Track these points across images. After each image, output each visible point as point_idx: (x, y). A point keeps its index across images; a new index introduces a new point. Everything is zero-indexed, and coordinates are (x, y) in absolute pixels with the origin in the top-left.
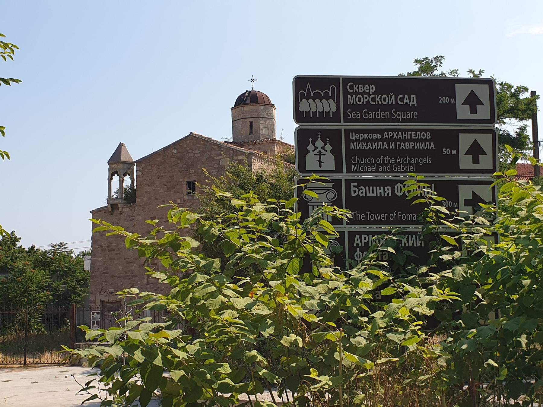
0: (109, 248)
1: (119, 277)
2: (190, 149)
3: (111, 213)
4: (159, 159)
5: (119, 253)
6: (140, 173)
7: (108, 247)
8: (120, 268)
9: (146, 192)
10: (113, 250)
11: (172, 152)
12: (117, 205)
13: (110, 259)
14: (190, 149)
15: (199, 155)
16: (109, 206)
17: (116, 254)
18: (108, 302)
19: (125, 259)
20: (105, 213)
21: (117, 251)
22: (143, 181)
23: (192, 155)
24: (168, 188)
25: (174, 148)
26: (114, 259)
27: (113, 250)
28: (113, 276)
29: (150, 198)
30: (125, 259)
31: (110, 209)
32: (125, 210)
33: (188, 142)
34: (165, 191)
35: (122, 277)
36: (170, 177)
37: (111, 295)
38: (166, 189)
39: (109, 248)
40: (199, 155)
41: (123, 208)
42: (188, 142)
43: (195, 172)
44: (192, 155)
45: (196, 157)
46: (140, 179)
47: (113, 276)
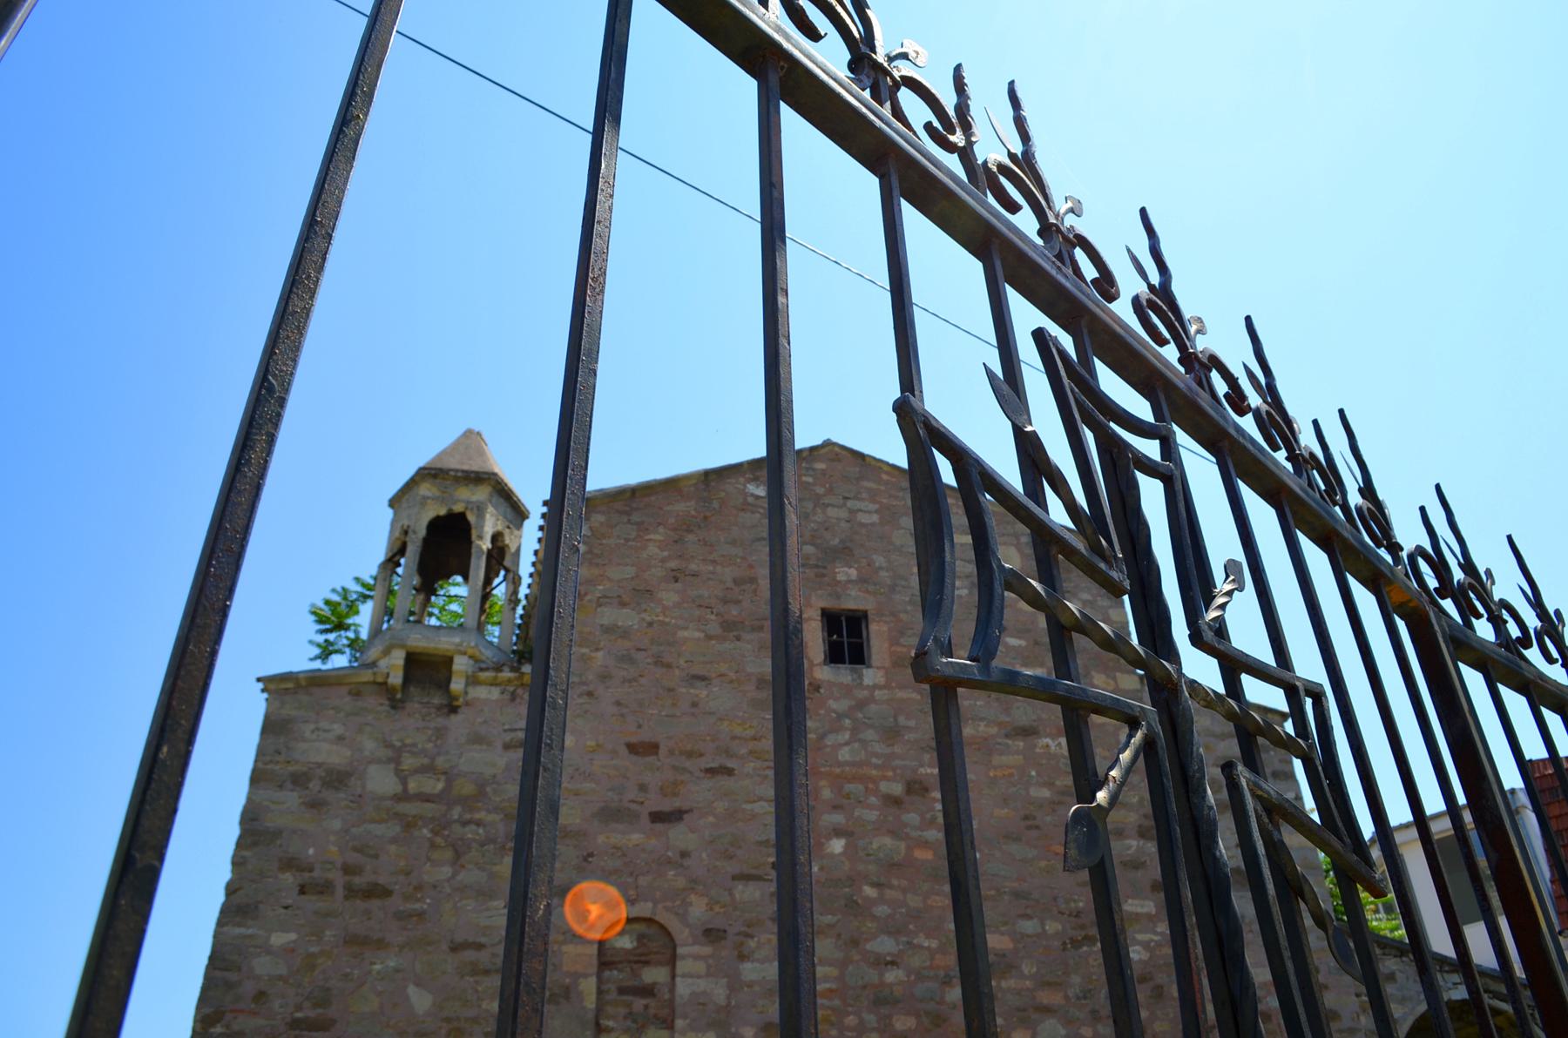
0: (357, 880)
2: (830, 491)
3: (395, 699)
4: (683, 507)
5: (421, 915)
7: (348, 870)
8: (421, 1000)
9: (608, 630)
10: (376, 892)
11: (745, 494)
12: (448, 661)
14: (830, 491)
15: (875, 518)
16: (398, 658)
17: (401, 916)
19: (455, 948)
20: (356, 693)
21: (407, 898)
22: (590, 582)
23: (843, 514)
24: (729, 626)
25: (755, 479)
26: (381, 944)
27: (376, 892)
29: (627, 659)
30: (455, 948)
31: (396, 679)
32: (480, 692)
33: (820, 466)
34: (709, 637)
36: (735, 581)
38: (714, 628)
39: (357, 880)
40: (875, 518)
41: (472, 681)
42: (820, 466)
43: (862, 580)
44: (843, 514)
45: (862, 525)
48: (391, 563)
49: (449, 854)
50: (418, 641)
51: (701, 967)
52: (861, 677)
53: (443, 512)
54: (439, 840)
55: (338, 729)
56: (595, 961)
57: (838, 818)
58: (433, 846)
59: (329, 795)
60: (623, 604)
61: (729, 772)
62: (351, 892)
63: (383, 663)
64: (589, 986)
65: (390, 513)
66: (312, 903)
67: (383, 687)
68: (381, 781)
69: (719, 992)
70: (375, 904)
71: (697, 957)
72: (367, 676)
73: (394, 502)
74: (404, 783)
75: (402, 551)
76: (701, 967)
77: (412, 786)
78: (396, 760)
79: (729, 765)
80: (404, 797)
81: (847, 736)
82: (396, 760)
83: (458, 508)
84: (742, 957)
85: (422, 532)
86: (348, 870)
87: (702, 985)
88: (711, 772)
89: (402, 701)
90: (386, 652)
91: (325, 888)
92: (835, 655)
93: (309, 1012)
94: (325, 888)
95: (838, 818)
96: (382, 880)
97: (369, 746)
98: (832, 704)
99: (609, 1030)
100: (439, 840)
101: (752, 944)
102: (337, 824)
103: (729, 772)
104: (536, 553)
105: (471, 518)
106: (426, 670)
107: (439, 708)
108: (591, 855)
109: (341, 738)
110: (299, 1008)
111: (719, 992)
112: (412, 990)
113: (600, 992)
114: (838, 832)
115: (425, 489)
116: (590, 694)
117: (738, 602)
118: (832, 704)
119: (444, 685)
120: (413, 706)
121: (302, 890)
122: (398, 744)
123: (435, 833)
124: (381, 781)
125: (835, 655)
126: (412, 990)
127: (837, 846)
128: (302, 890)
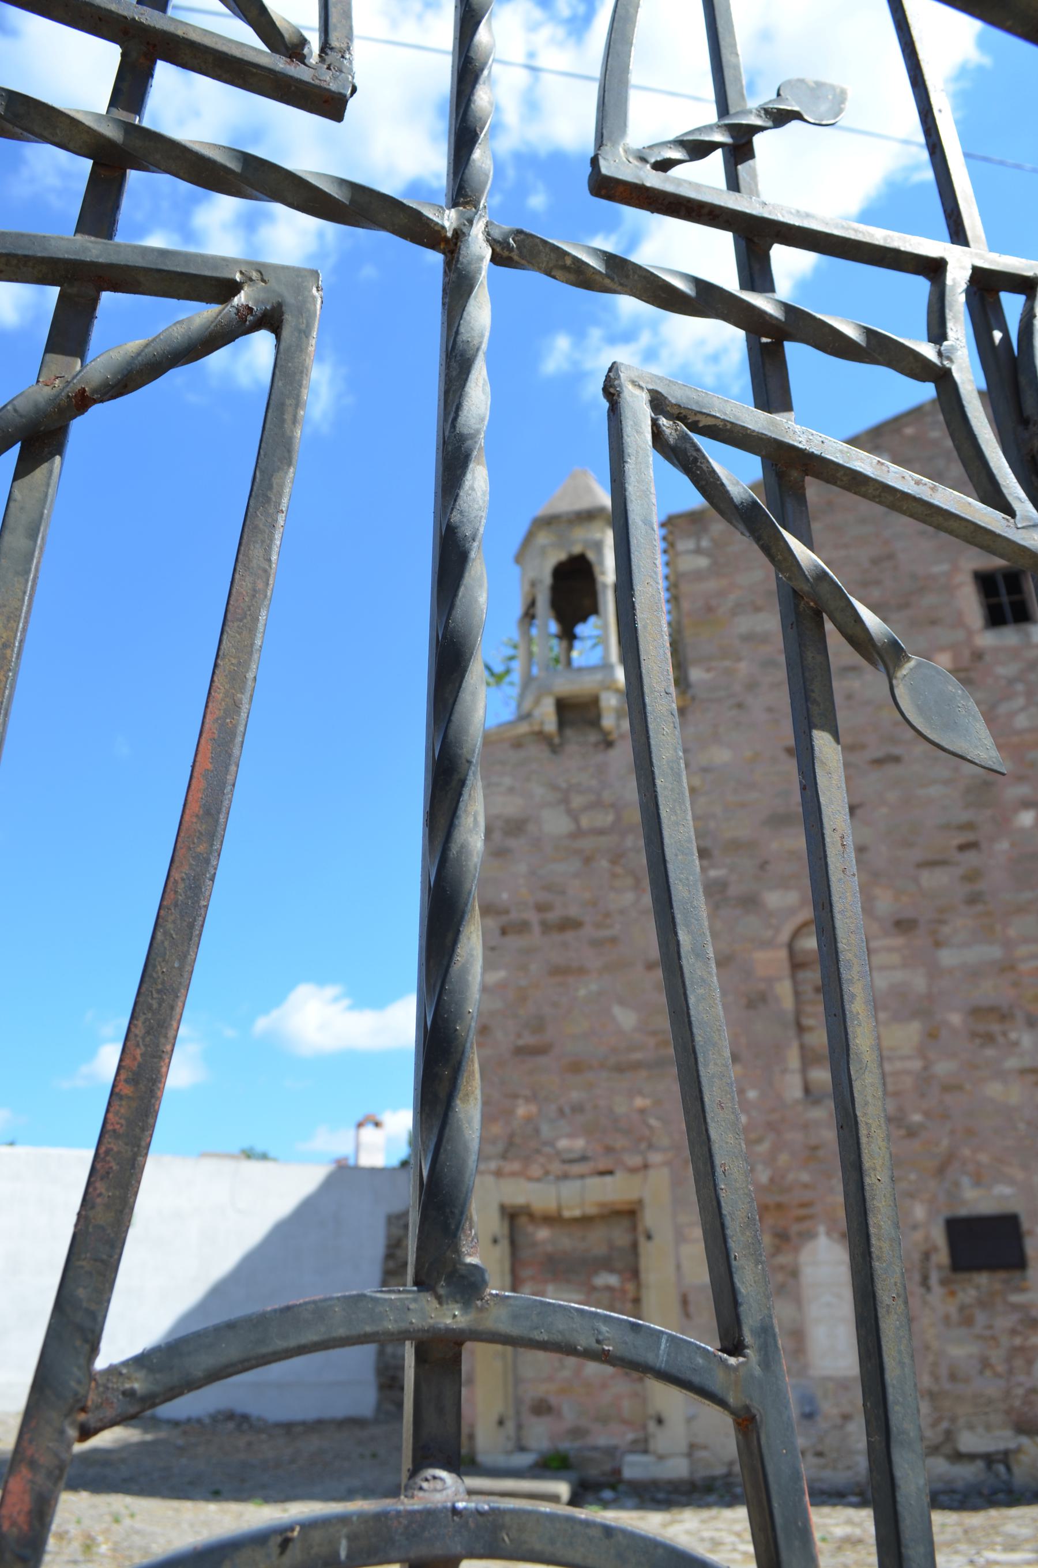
1: (620, 1069)
5: (613, 940)
6: (703, 562)
7: (541, 908)
10: (568, 924)
13: (560, 971)
17: (596, 944)
18: (553, 1220)
21: (598, 926)
26: (581, 971)
27: (568, 924)
28: (576, 1067)
31: (551, 725)
35: (636, 1066)
37: (576, 1169)
46: (712, 585)
47: (576, 1067)
48: (529, 615)
49: (629, 881)
50: (566, 685)
51: (895, 958)
52: (1028, 635)
53: (563, 556)
54: (619, 870)
55: (507, 781)
56: (786, 965)
57: (1023, 790)
58: (614, 876)
59: (512, 843)
60: (757, 609)
61: (896, 759)
62: (547, 928)
63: (537, 713)
64: (784, 990)
65: (515, 571)
66: (514, 942)
67: (541, 736)
68: (555, 823)
69: (919, 982)
70: (569, 936)
71: (890, 950)
72: (523, 728)
73: (519, 558)
74: (576, 819)
75: (532, 604)
76: (895, 958)
77: (585, 822)
78: (565, 801)
79: (897, 751)
80: (578, 833)
81: (1021, 701)
82: (565, 801)
83: (577, 549)
84: (938, 944)
85: (547, 579)
86: (541, 908)
87: (899, 976)
88: (879, 762)
89: (561, 745)
90: (537, 702)
91: (522, 927)
92: (995, 618)
93: (529, 1039)
94: (522, 927)
95: (1023, 790)
96: (573, 911)
97: (539, 791)
98: (1001, 671)
99: (810, 1029)
100: (619, 870)
101: (946, 930)
102: (522, 868)
103: (896, 759)
104: (667, 578)
105: (591, 556)
106: (576, 713)
107: (596, 745)
108: (766, 863)
109: (511, 790)
110: (519, 1036)
111: (919, 982)
112: (618, 1011)
113: (797, 994)
114: (1027, 804)
115: (543, 538)
116: (740, 706)
117: (878, 583)
118: (1001, 671)
119: (595, 722)
120: (572, 748)
121: (504, 932)
122: (564, 785)
123: (614, 862)
124: (555, 823)
125: (995, 618)
126: (618, 1011)
127: (1026, 818)
128: (504, 932)
